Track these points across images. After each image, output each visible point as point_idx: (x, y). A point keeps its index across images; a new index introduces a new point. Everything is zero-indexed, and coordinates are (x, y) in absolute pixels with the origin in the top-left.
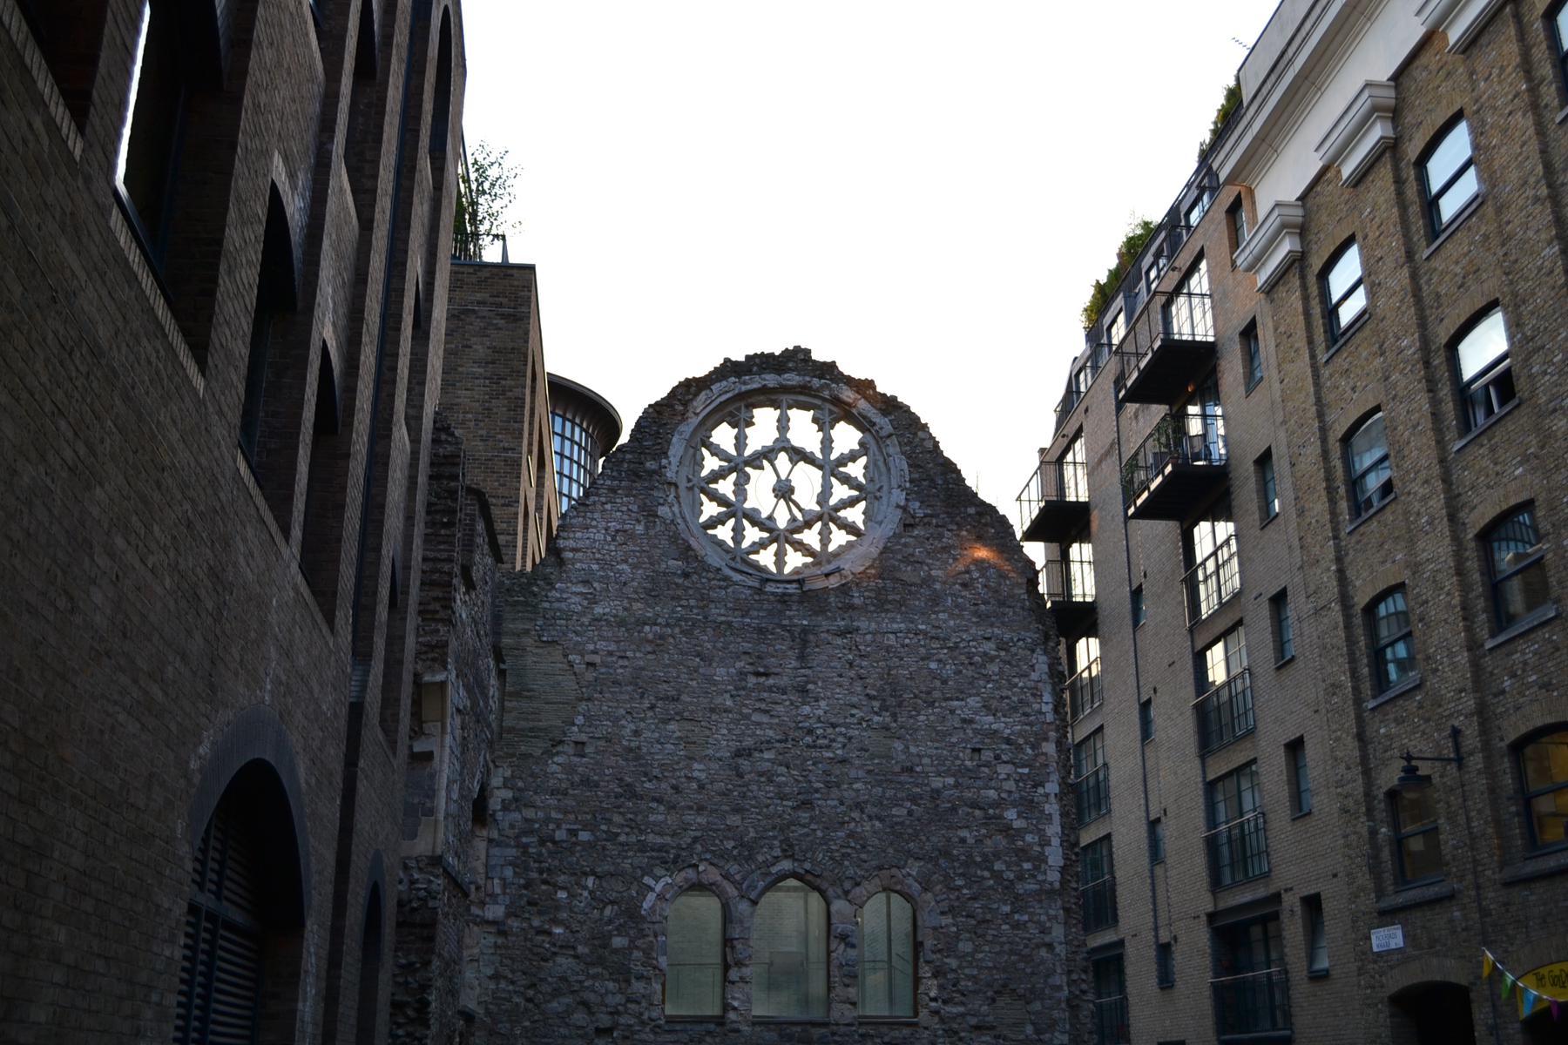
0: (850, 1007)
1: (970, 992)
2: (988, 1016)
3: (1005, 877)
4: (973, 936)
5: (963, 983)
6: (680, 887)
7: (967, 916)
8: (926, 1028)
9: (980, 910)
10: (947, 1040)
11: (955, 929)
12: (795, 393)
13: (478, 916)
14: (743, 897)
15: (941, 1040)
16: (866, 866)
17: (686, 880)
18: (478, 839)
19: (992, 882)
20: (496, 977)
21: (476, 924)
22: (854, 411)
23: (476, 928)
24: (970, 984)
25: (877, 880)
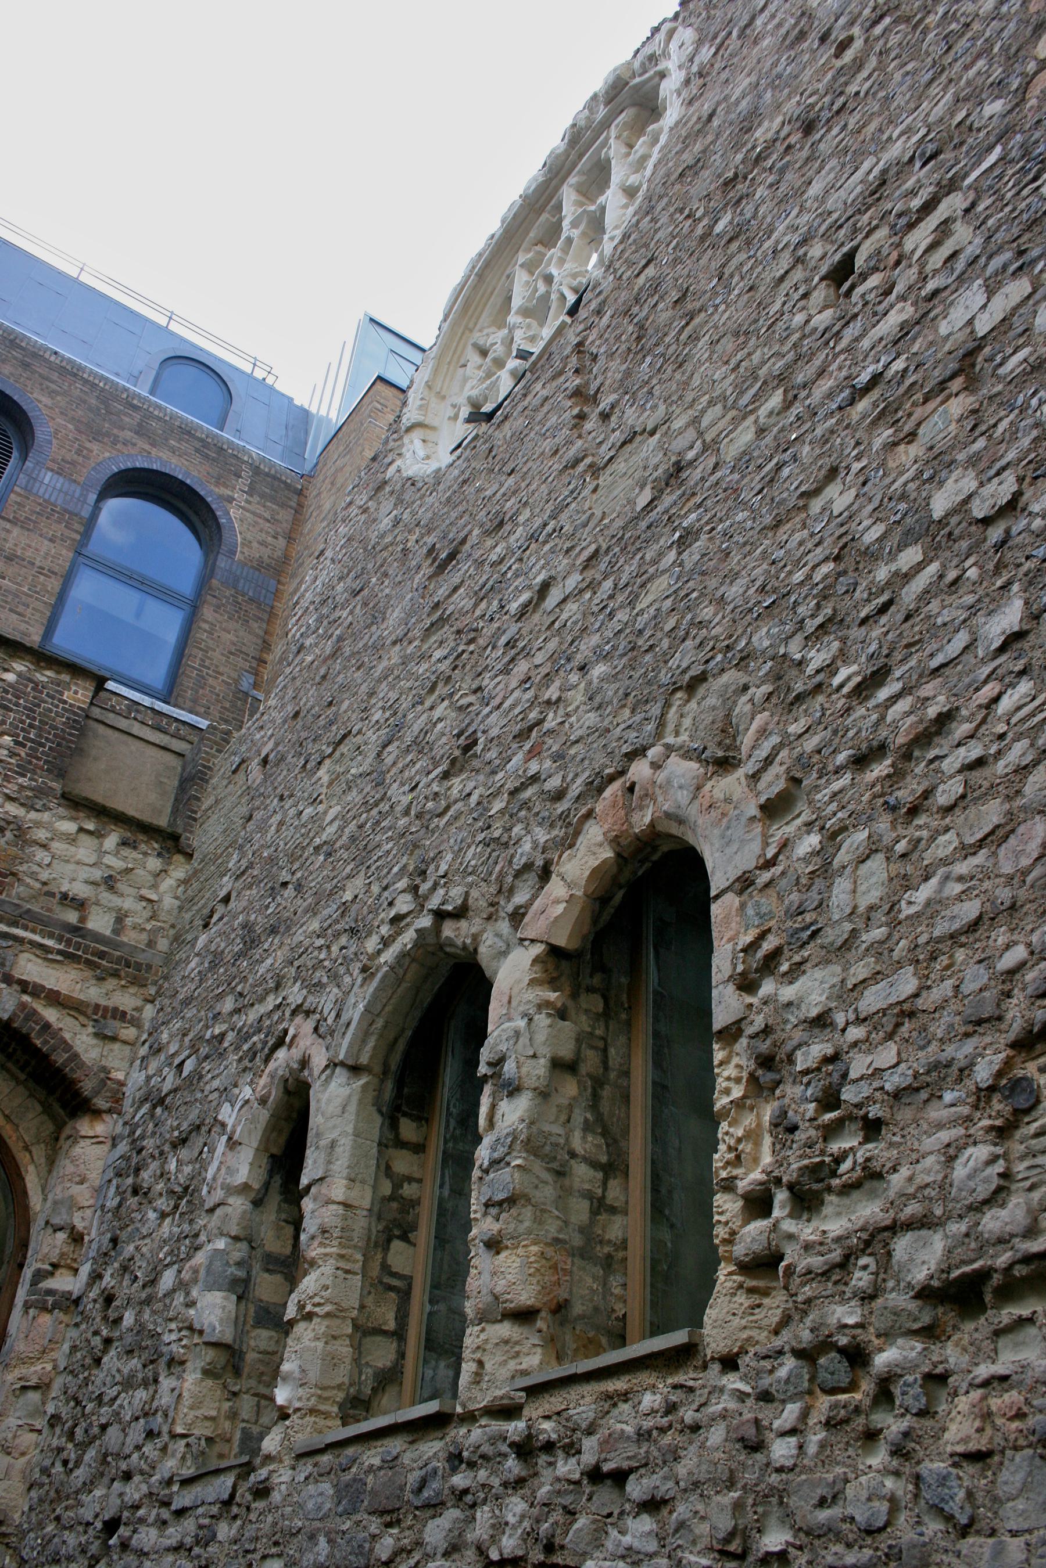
0: (505, 1329)
1: (897, 1095)
2: (997, 1197)
3: (979, 510)
4: (883, 824)
5: (859, 1065)
6: (263, 1101)
7: (861, 761)
8: (729, 1363)
9: (903, 705)
10: (823, 1403)
11: (814, 840)
12: (574, 165)
13: (50, 1292)
14: (336, 1065)
15: (791, 1412)
16: (561, 807)
17: (272, 1076)
18: (82, 1143)
19: (933, 568)
20: (55, 1420)
21: (45, 1309)
22: (637, 80)
23: (46, 1319)
24: (887, 1055)
25: (594, 833)
